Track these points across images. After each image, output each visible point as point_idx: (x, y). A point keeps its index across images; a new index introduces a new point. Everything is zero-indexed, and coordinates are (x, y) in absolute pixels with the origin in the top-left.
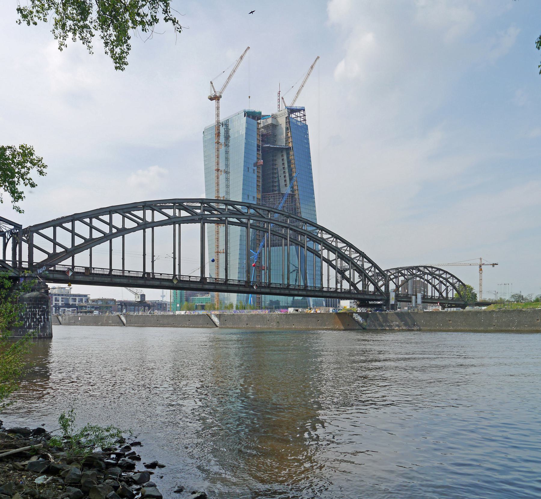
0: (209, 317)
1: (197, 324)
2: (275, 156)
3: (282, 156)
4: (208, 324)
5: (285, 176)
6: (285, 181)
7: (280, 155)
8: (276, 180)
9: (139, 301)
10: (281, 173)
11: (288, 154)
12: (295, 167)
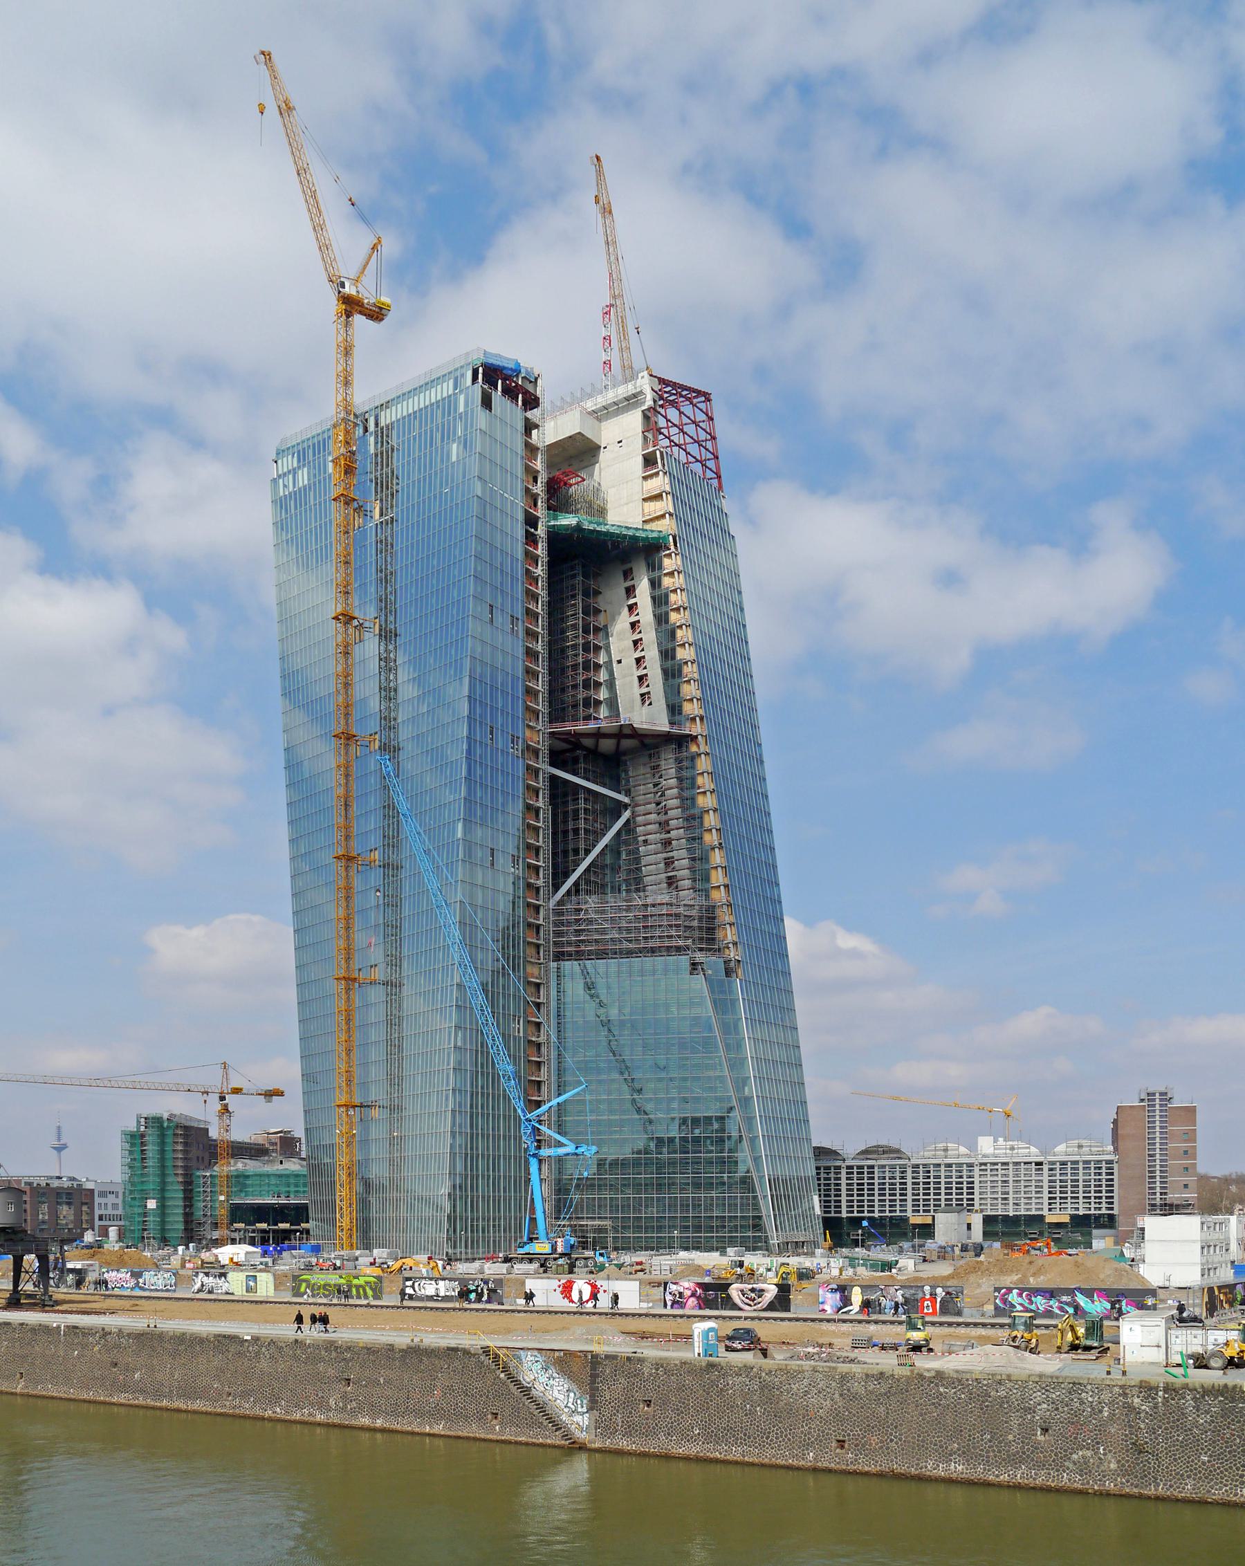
0: (505, 1369)
8: (603, 676)
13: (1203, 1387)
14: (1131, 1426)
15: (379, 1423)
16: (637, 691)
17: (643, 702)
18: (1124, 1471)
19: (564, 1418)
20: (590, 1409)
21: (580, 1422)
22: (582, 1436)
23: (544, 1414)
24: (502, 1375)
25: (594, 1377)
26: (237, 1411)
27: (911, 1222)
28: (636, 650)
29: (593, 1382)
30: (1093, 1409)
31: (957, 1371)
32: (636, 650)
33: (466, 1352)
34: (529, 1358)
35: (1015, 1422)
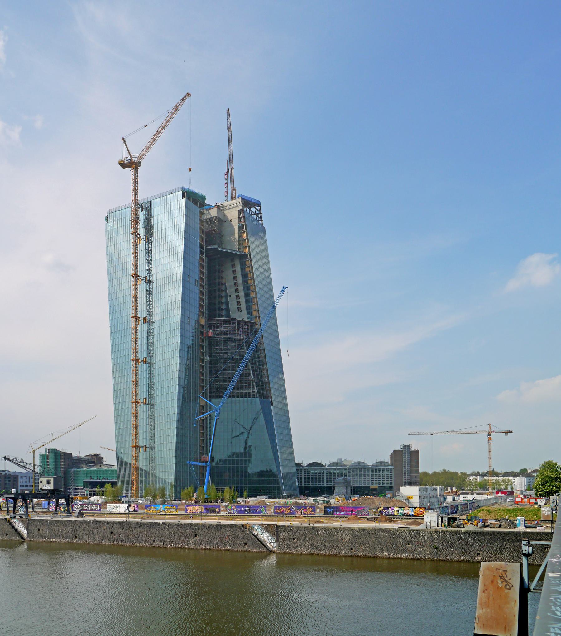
1: (217, 544)
2: (223, 265)
3: (233, 266)
4: (246, 544)
5: (237, 296)
6: (238, 303)
7: (229, 265)
8: (223, 300)
9: (49, 488)
10: (231, 291)
11: (243, 265)
12: (254, 283)
13: (451, 531)
14: (433, 542)
15: (207, 547)
16: (236, 306)
17: (238, 311)
18: (431, 554)
19: (268, 544)
20: (276, 541)
21: (273, 544)
22: (274, 549)
23: (261, 542)
24: (248, 532)
25: (277, 532)
26: (158, 546)
27: (371, 488)
28: (236, 293)
29: (277, 533)
30: (423, 537)
31: (385, 528)
32: (236, 293)
33: (236, 526)
34: (256, 527)
35: (401, 541)
